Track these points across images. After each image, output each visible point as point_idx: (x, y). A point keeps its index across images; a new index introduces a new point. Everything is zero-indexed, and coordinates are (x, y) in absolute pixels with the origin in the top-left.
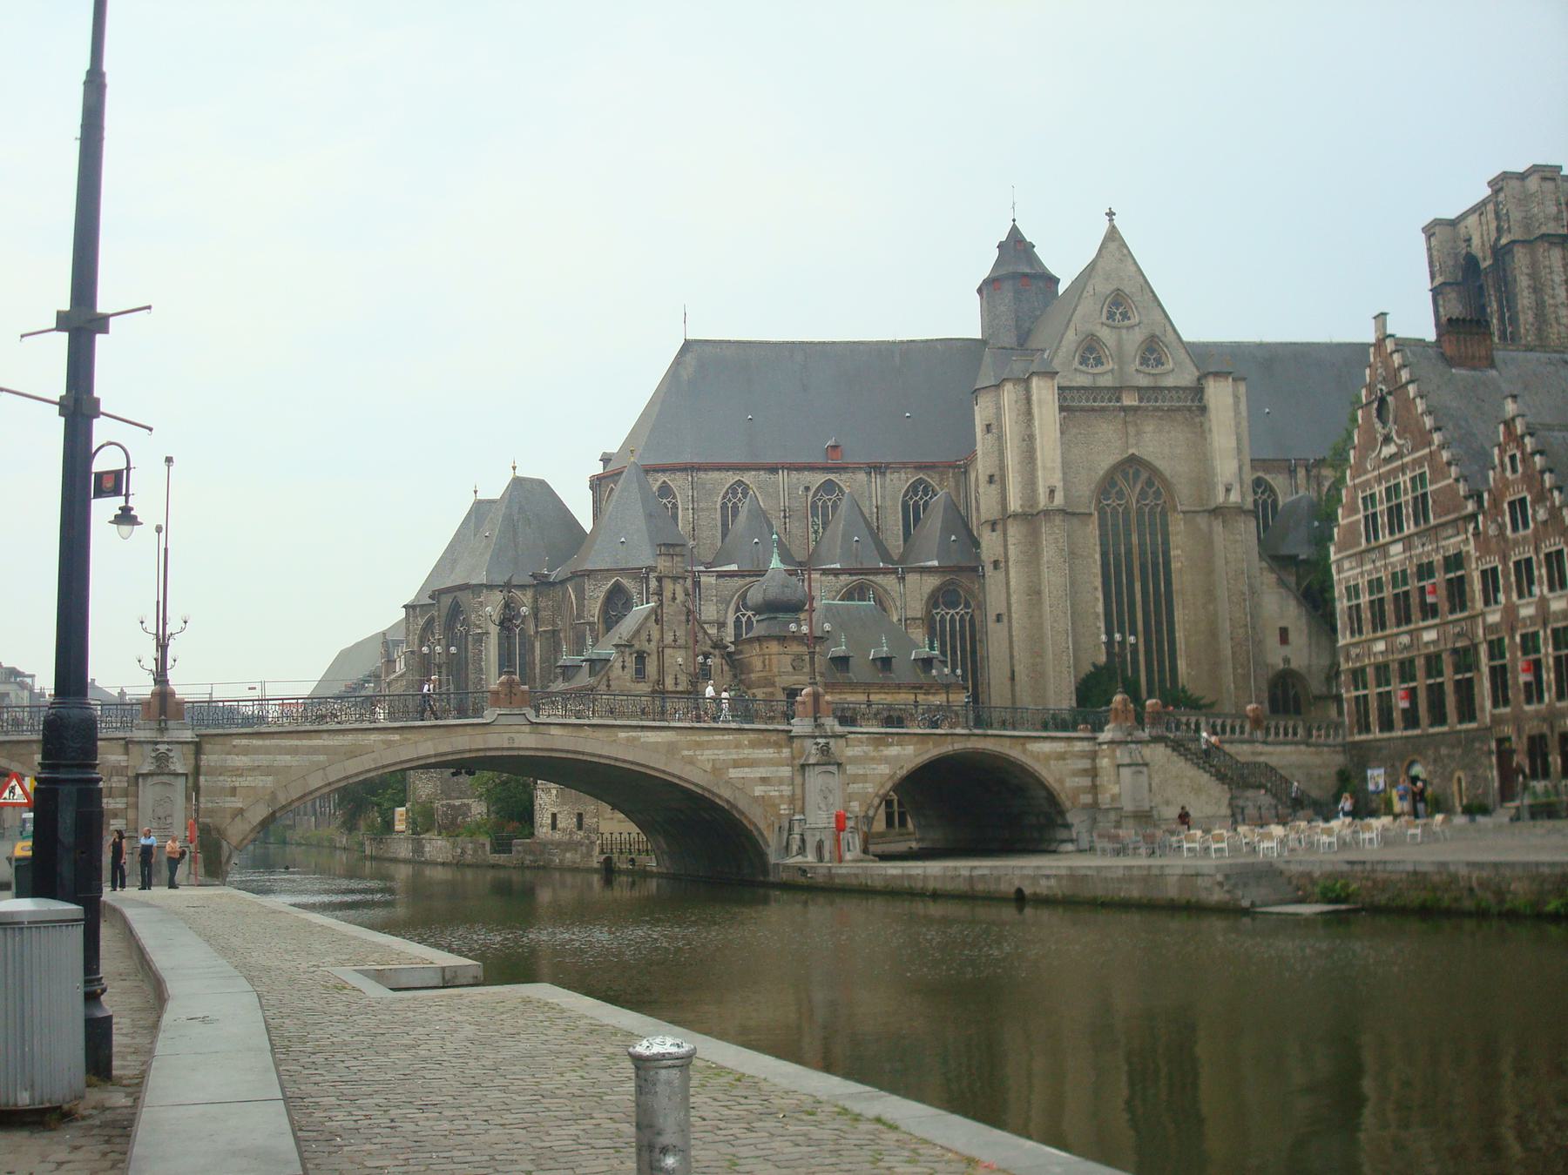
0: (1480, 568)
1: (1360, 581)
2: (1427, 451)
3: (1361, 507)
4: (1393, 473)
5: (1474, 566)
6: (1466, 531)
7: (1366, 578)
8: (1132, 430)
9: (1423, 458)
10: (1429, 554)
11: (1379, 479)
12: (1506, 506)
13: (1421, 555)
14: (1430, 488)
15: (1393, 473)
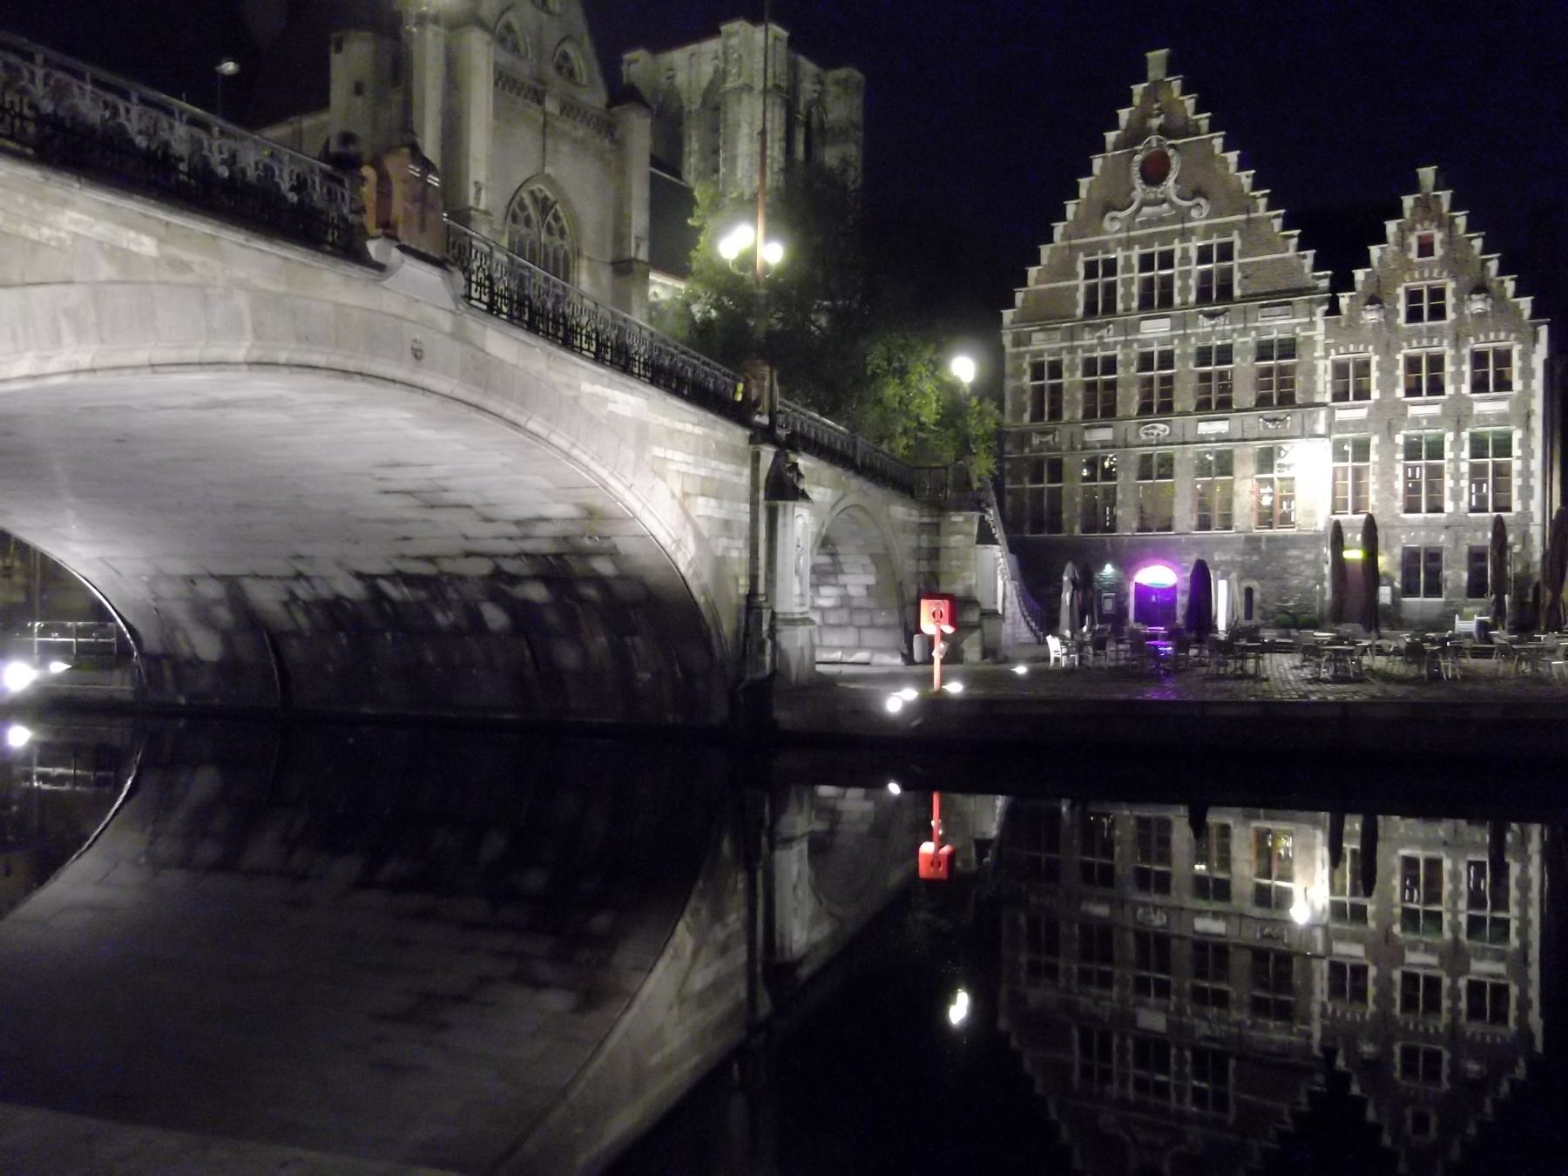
0: (1333, 356)
1: (1066, 358)
2: (1243, 217)
3: (1081, 271)
4: (1166, 238)
5: (1319, 353)
6: (1312, 314)
7: (1081, 355)
8: (550, 143)
9: (1233, 225)
10: (1224, 336)
11: (1128, 244)
12: (1401, 291)
13: (1207, 336)
14: (1237, 261)
15: (1166, 238)
